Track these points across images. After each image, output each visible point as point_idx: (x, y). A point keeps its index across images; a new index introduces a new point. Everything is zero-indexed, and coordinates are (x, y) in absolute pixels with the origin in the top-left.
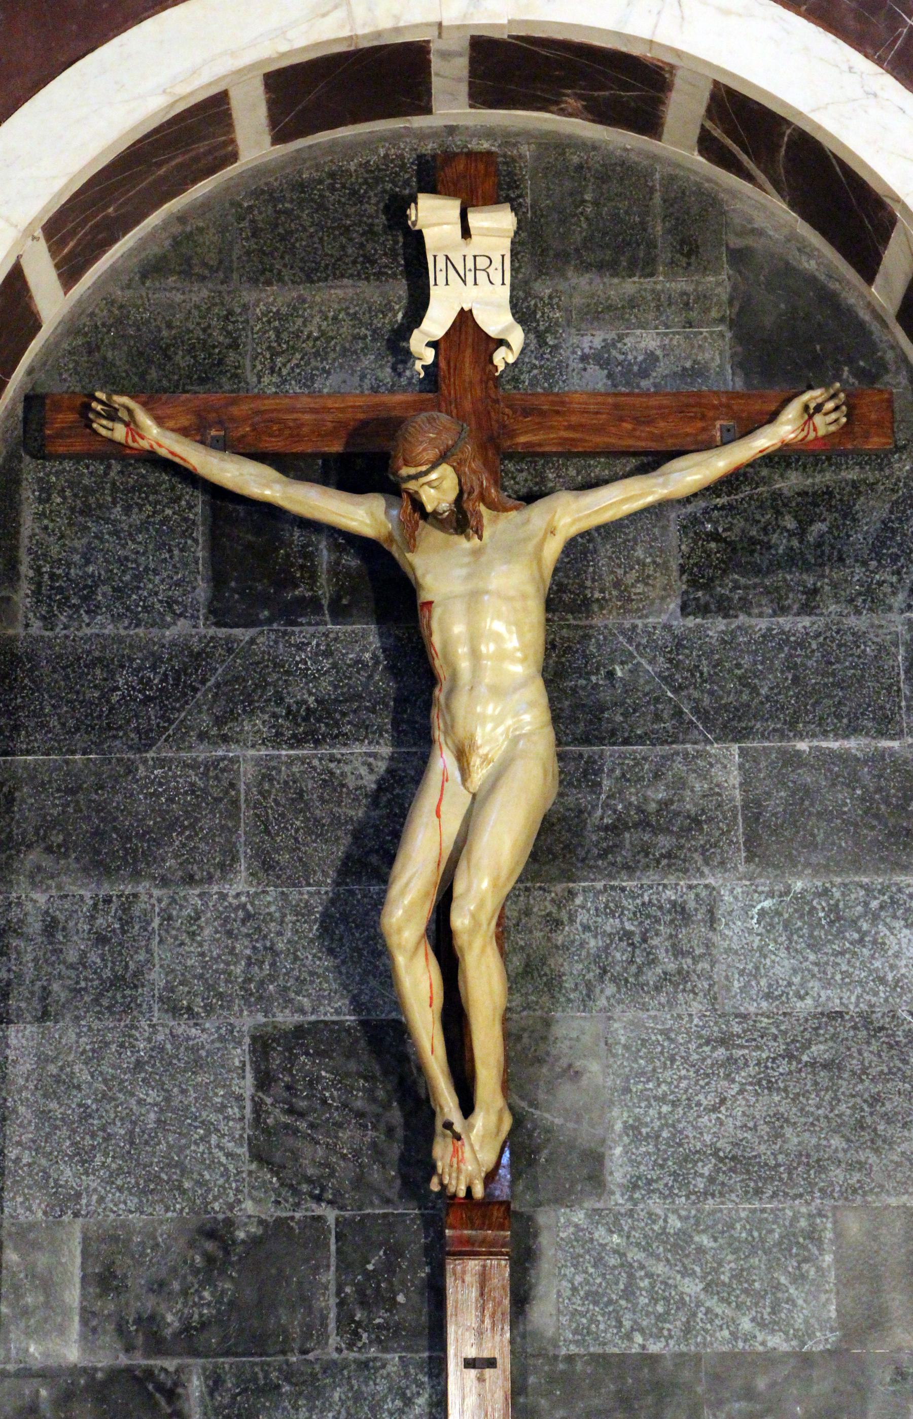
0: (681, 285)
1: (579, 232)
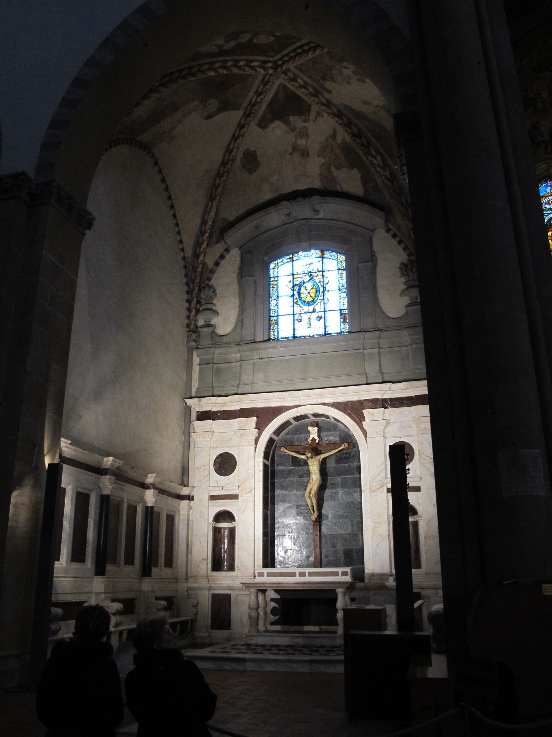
0: (334, 433)
1: (325, 428)
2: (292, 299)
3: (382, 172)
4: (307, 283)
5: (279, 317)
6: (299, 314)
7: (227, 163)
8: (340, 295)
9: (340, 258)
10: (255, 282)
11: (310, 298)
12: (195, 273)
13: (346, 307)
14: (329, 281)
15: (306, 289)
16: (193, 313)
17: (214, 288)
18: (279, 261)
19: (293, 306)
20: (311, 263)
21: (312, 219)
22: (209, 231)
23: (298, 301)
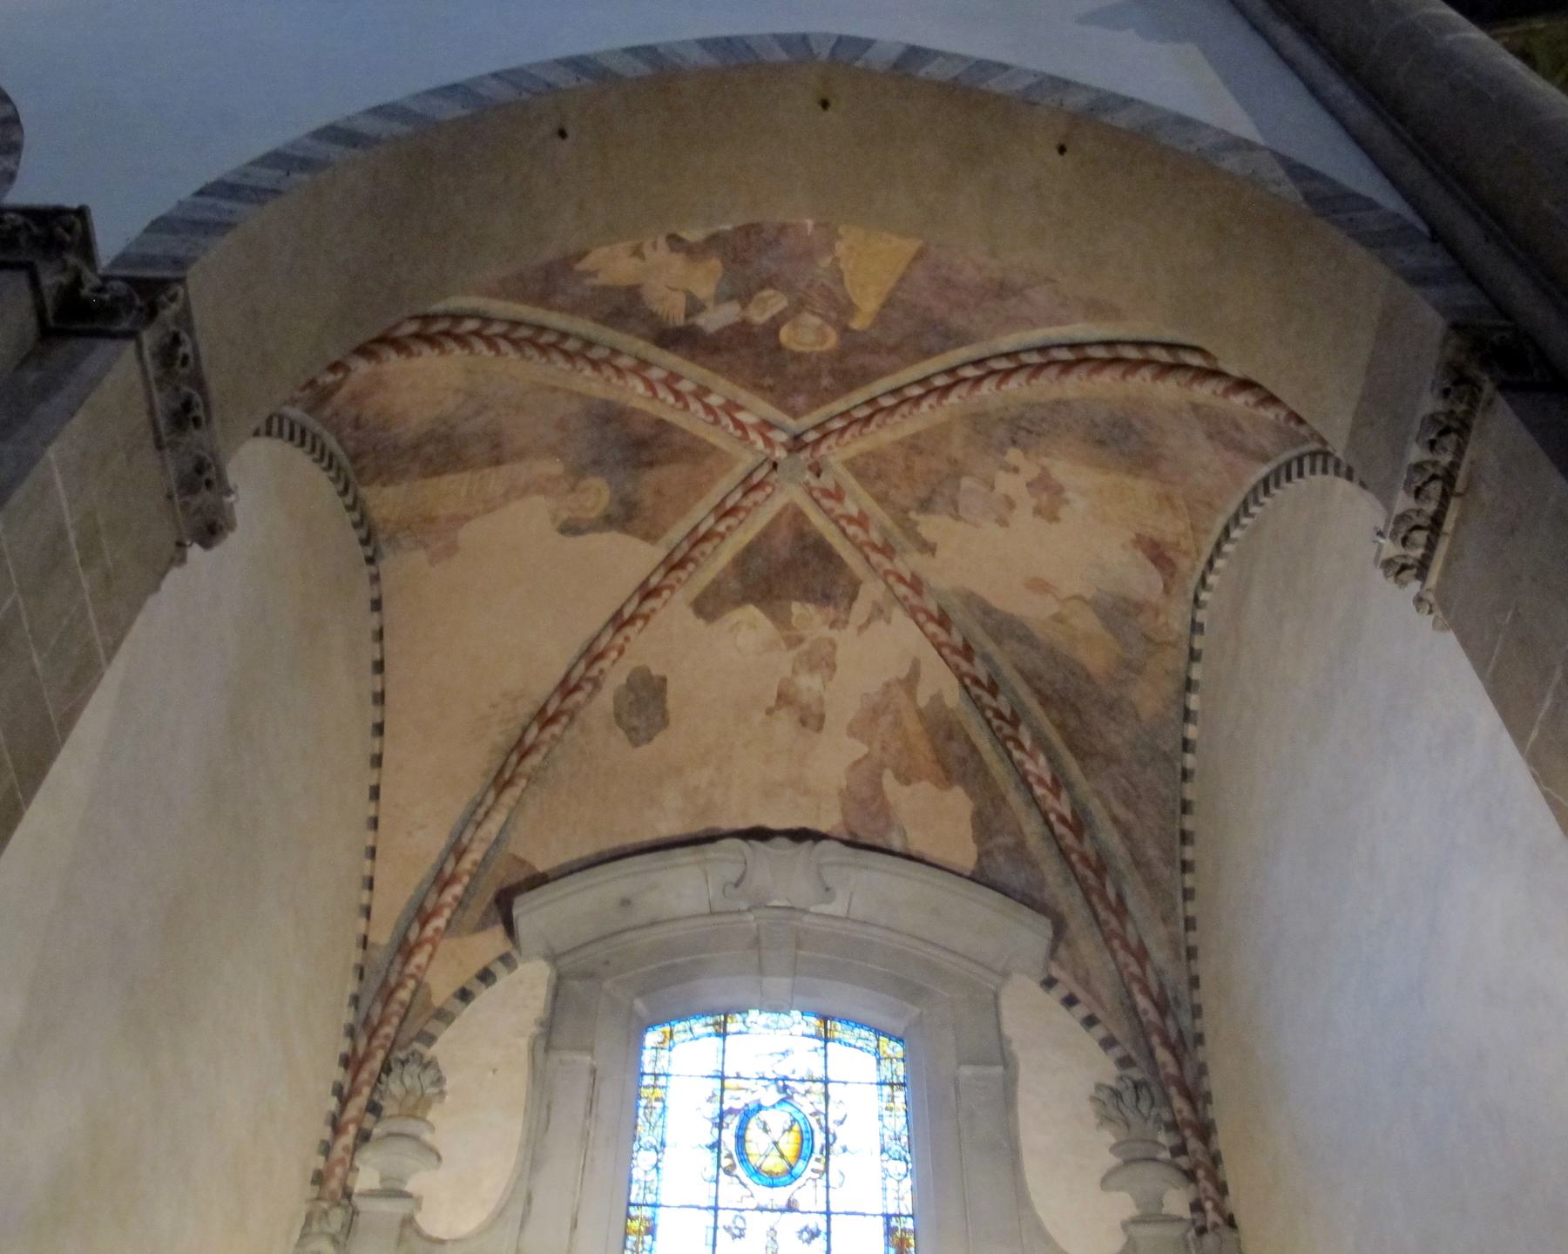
2: (711, 1156)
3: (1050, 801)
4: (772, 1111)
5: (661, 1208)
6: (735, 1209)
7: (577, 688)
8: (885, 1165)
9: (886, 1048)
10: (593, 1071)
11: (780, 1160)
12: (386, 1004)
13: (906, 1206)
14: (846, 1116)
15: (766, 1130)
16: (347, 1139)
17: (439, 1071)
18: (679, 1026)
19: (717, 1182)
20: (787, 1051)
21: (805, 911)
22: (466, 879)
23: (733, 1166)
